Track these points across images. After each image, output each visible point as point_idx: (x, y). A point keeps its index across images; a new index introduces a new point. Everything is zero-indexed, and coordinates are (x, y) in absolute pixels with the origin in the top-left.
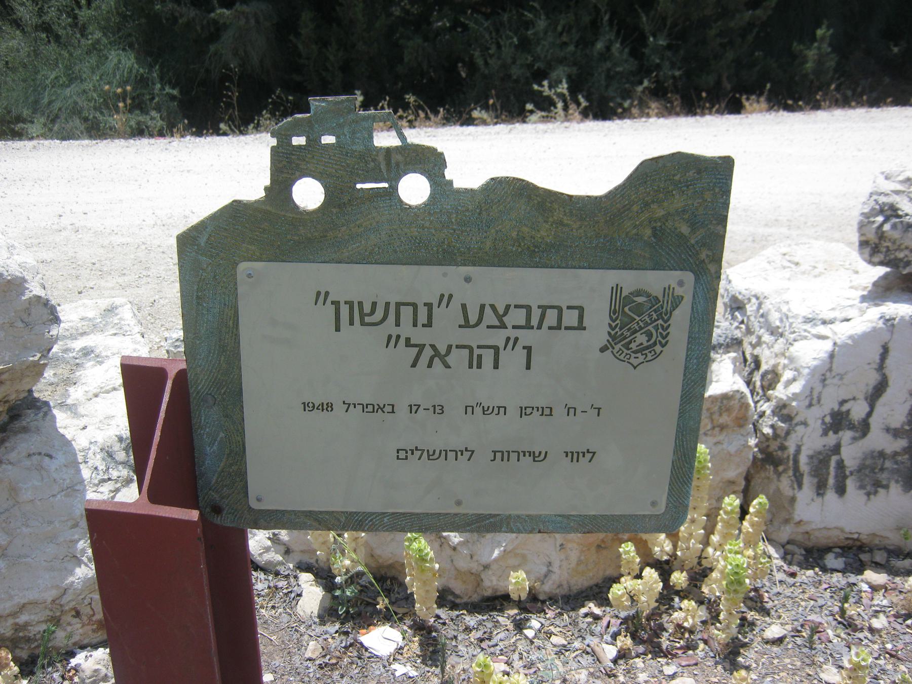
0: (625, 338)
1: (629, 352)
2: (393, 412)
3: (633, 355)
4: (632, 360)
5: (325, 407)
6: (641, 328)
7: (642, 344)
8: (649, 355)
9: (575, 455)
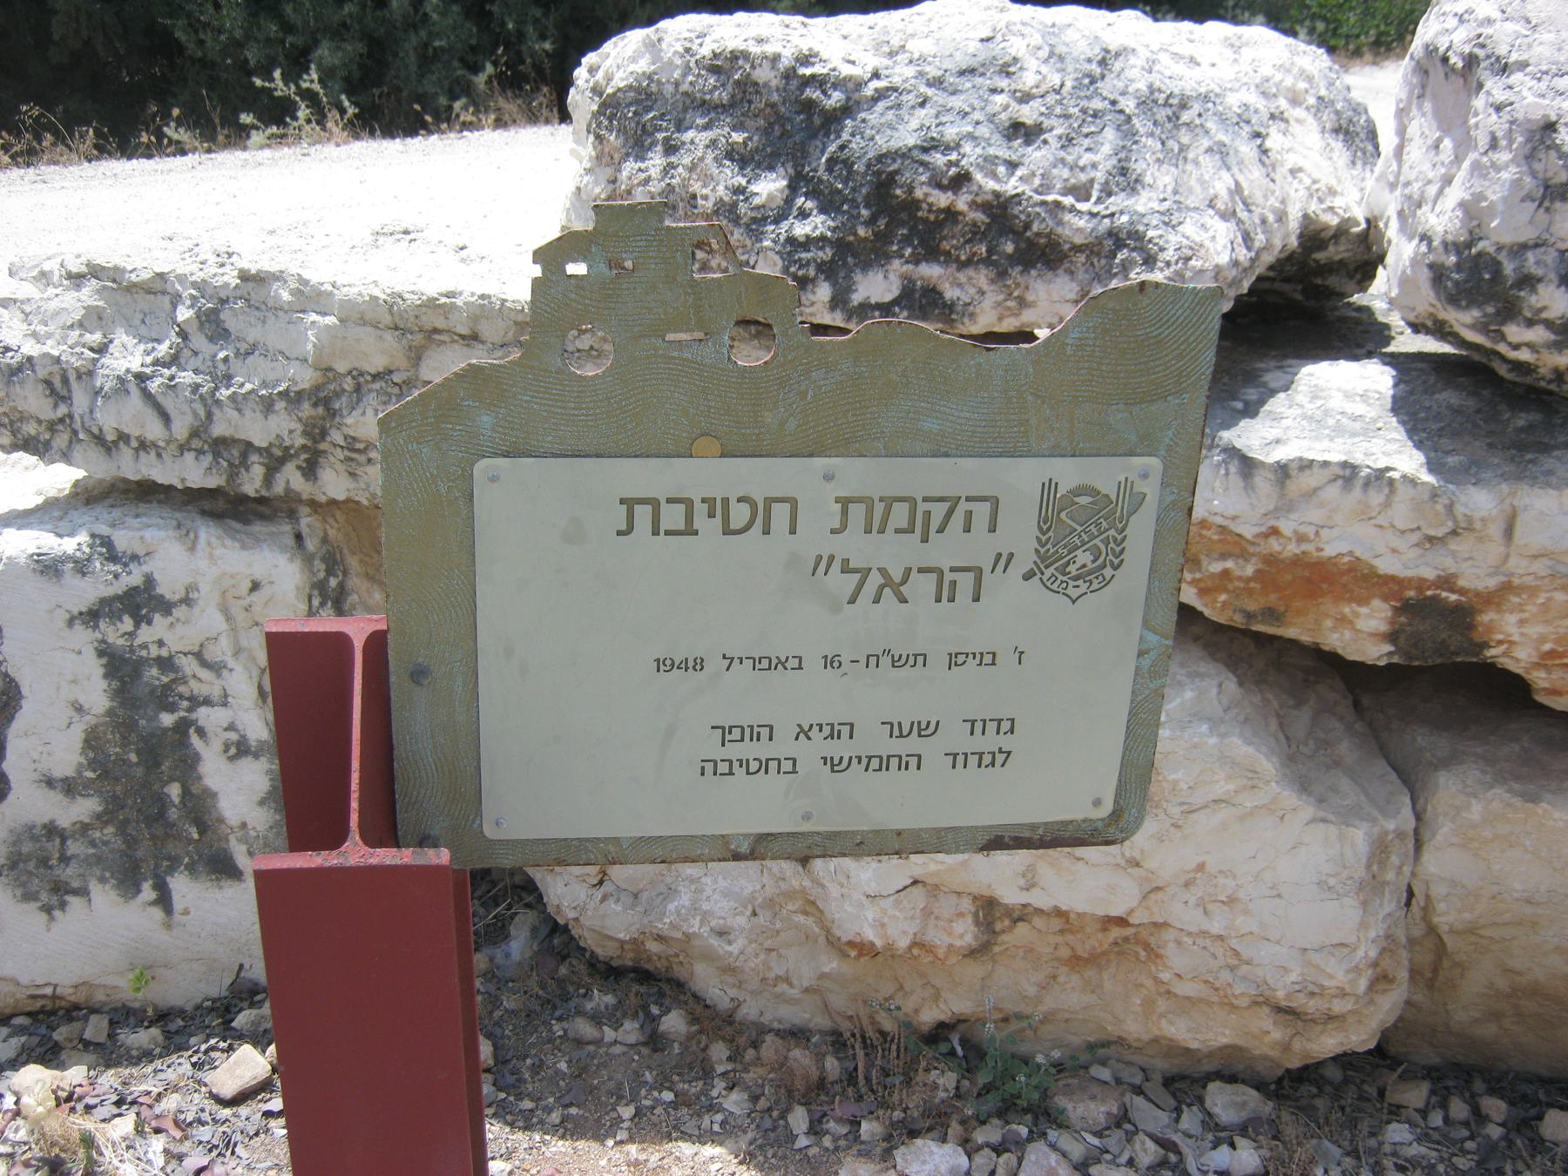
3: (1071, 583)
5: (691, 664)
7: (1084, 566)
8: (1095, 582)
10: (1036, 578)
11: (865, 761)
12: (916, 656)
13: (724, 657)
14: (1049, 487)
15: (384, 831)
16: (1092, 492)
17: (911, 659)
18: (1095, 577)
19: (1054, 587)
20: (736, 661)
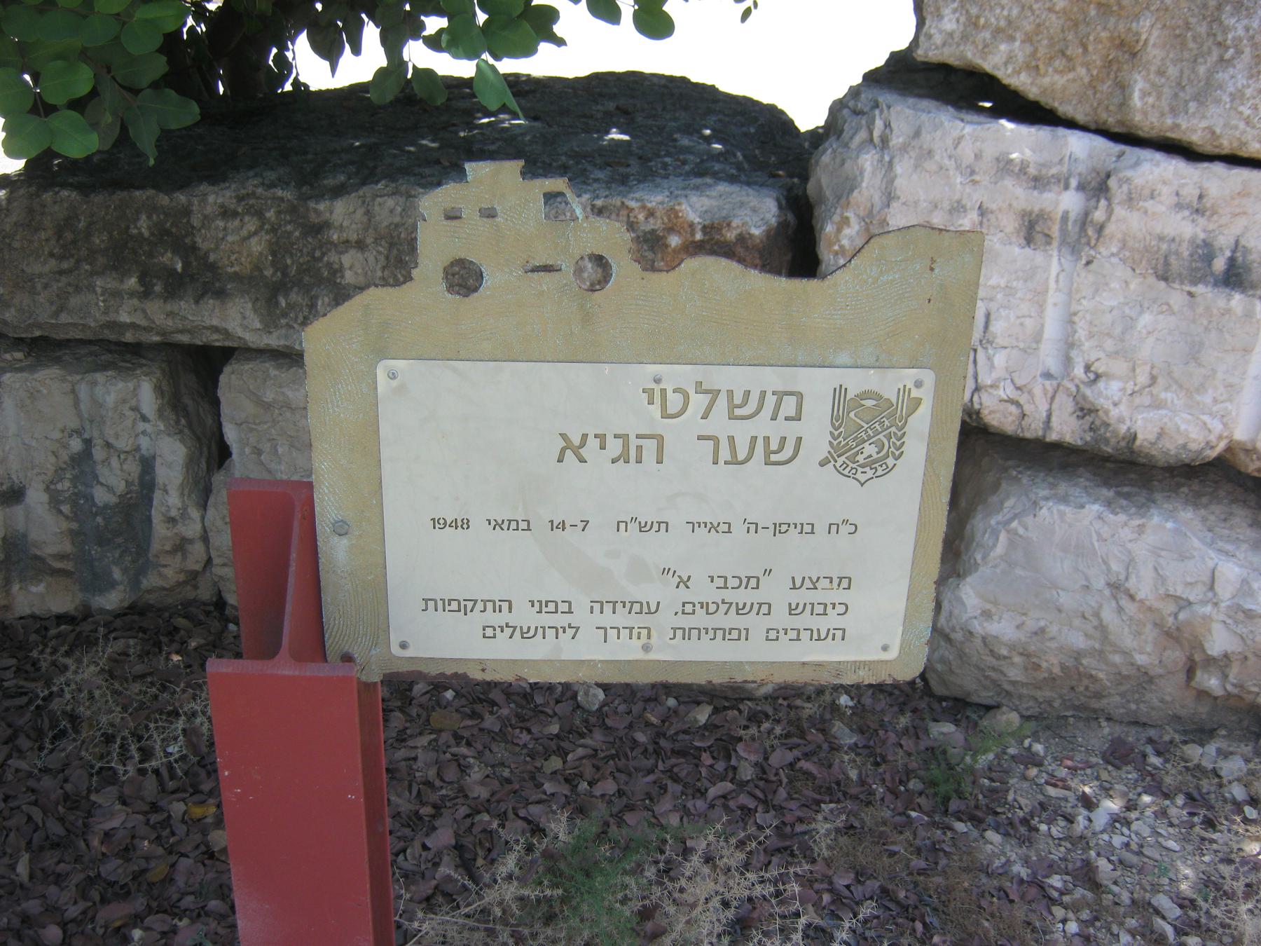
0: (851, 449)
3: (860, 470)
4: (859, 476)
6: (870, 438)
7: (870, 456)
10: (830, 465)
11: (628, 605)
14: (840, 392)
16: (878, 397)
19: (846, 472)
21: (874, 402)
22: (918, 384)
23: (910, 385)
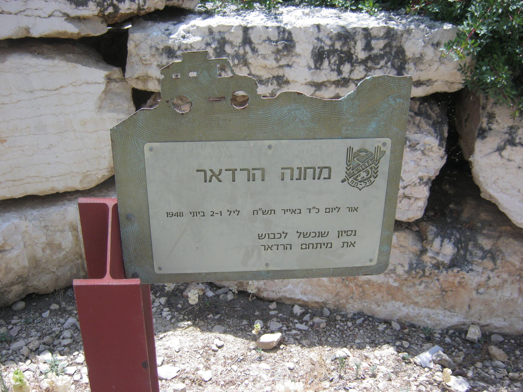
1: (357, 182)
2: (300, 213)
3: (359, 183)
4: (359, 186)
6: (363, 169)
7: (363, 177)
8: (368, 183)
9: (340, 233)
10: (346, 182)
12: (271, 210)
13: (228, 211)
15: (120, 271)
16: (366, 151)
17: (270, 212)
18: (368, 181)
19: (353, 185)
20: (232, 212)
21: (365, 153)
22: (384, 144)
23: (380, 145)
